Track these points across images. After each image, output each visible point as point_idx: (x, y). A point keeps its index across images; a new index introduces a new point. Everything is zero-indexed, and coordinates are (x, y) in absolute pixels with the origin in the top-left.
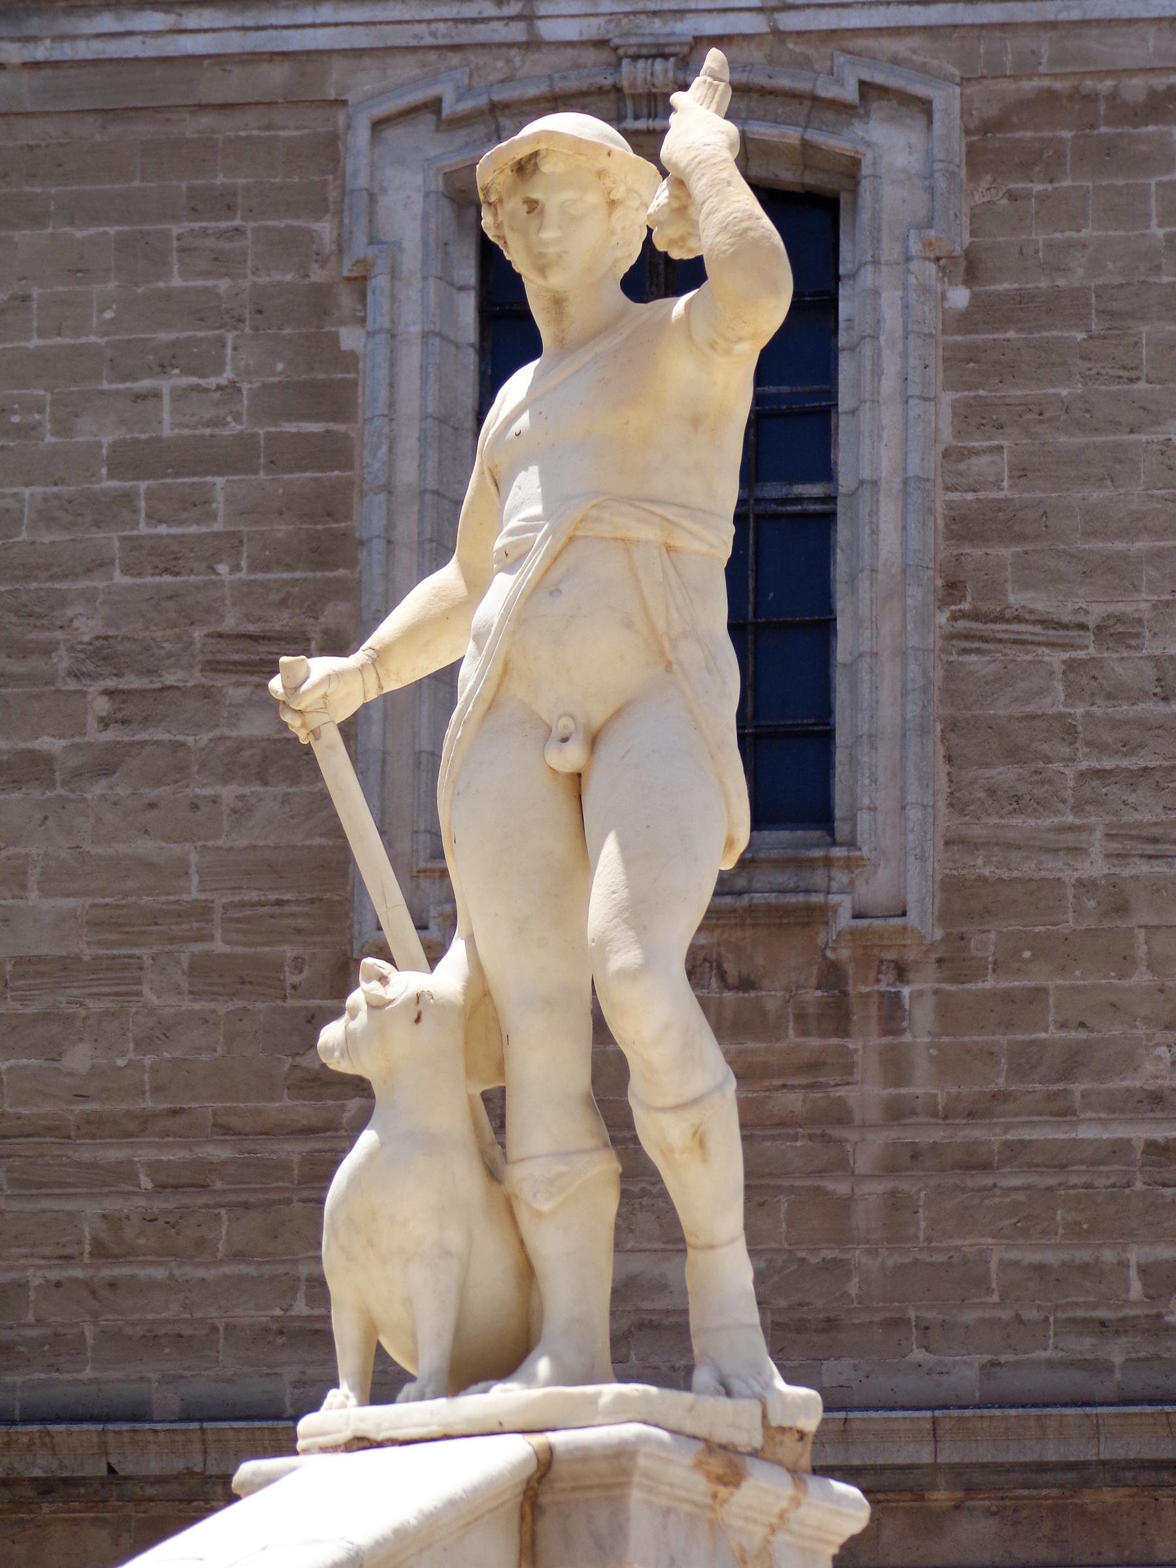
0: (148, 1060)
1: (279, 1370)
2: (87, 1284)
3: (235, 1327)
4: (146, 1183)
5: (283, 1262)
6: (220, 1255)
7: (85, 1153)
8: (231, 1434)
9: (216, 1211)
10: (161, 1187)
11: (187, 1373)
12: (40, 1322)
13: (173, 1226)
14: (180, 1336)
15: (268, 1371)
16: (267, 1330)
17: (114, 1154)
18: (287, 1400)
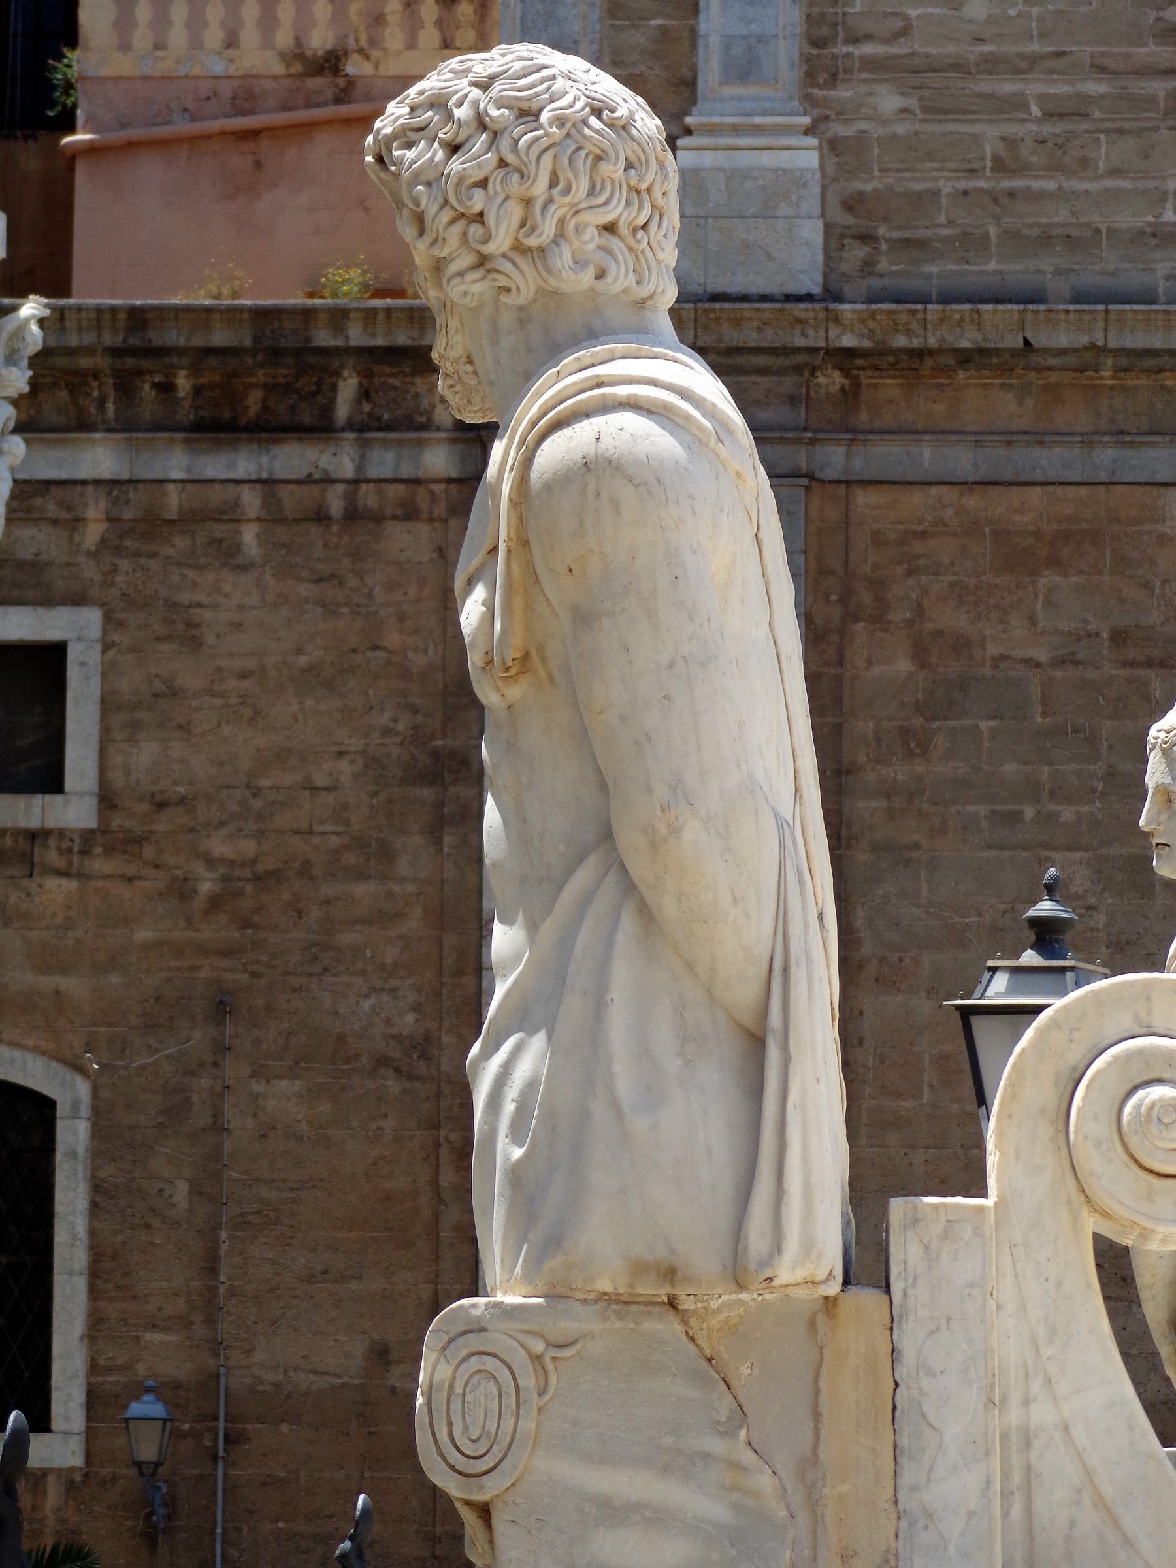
0: (1035, 11)
1: (1153, 266)
2: (989, 192)
3: (1115, 230)
4: (1036, 111)
5: (1153, 178)
6: (1100, 171)
7: (985, 86)
8: (1130, 316)
9: (1096, 135)
10: (1048, 116)
11: (1076, 267)
12: (951, 223)
13: (1061, 147)
14: (1069, 237)
15: (1144, 266)
16: (1142, 233)
17: (1008, 87)
18: (1161, 291)
